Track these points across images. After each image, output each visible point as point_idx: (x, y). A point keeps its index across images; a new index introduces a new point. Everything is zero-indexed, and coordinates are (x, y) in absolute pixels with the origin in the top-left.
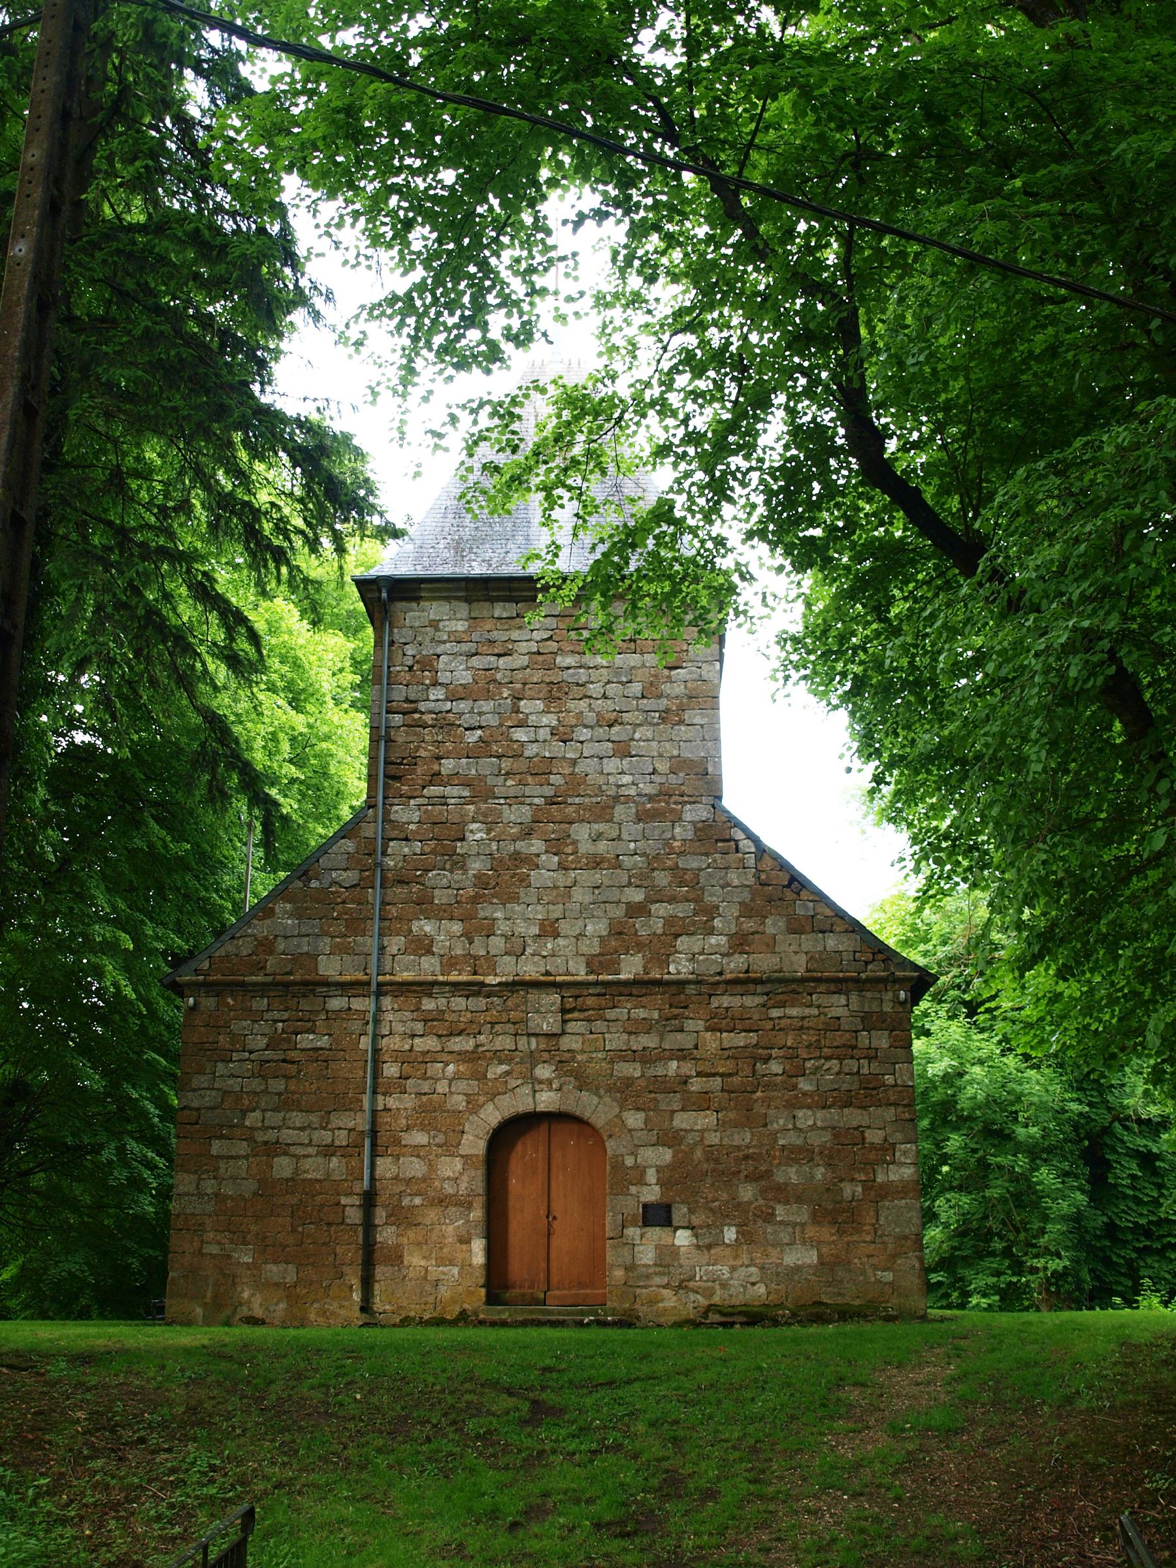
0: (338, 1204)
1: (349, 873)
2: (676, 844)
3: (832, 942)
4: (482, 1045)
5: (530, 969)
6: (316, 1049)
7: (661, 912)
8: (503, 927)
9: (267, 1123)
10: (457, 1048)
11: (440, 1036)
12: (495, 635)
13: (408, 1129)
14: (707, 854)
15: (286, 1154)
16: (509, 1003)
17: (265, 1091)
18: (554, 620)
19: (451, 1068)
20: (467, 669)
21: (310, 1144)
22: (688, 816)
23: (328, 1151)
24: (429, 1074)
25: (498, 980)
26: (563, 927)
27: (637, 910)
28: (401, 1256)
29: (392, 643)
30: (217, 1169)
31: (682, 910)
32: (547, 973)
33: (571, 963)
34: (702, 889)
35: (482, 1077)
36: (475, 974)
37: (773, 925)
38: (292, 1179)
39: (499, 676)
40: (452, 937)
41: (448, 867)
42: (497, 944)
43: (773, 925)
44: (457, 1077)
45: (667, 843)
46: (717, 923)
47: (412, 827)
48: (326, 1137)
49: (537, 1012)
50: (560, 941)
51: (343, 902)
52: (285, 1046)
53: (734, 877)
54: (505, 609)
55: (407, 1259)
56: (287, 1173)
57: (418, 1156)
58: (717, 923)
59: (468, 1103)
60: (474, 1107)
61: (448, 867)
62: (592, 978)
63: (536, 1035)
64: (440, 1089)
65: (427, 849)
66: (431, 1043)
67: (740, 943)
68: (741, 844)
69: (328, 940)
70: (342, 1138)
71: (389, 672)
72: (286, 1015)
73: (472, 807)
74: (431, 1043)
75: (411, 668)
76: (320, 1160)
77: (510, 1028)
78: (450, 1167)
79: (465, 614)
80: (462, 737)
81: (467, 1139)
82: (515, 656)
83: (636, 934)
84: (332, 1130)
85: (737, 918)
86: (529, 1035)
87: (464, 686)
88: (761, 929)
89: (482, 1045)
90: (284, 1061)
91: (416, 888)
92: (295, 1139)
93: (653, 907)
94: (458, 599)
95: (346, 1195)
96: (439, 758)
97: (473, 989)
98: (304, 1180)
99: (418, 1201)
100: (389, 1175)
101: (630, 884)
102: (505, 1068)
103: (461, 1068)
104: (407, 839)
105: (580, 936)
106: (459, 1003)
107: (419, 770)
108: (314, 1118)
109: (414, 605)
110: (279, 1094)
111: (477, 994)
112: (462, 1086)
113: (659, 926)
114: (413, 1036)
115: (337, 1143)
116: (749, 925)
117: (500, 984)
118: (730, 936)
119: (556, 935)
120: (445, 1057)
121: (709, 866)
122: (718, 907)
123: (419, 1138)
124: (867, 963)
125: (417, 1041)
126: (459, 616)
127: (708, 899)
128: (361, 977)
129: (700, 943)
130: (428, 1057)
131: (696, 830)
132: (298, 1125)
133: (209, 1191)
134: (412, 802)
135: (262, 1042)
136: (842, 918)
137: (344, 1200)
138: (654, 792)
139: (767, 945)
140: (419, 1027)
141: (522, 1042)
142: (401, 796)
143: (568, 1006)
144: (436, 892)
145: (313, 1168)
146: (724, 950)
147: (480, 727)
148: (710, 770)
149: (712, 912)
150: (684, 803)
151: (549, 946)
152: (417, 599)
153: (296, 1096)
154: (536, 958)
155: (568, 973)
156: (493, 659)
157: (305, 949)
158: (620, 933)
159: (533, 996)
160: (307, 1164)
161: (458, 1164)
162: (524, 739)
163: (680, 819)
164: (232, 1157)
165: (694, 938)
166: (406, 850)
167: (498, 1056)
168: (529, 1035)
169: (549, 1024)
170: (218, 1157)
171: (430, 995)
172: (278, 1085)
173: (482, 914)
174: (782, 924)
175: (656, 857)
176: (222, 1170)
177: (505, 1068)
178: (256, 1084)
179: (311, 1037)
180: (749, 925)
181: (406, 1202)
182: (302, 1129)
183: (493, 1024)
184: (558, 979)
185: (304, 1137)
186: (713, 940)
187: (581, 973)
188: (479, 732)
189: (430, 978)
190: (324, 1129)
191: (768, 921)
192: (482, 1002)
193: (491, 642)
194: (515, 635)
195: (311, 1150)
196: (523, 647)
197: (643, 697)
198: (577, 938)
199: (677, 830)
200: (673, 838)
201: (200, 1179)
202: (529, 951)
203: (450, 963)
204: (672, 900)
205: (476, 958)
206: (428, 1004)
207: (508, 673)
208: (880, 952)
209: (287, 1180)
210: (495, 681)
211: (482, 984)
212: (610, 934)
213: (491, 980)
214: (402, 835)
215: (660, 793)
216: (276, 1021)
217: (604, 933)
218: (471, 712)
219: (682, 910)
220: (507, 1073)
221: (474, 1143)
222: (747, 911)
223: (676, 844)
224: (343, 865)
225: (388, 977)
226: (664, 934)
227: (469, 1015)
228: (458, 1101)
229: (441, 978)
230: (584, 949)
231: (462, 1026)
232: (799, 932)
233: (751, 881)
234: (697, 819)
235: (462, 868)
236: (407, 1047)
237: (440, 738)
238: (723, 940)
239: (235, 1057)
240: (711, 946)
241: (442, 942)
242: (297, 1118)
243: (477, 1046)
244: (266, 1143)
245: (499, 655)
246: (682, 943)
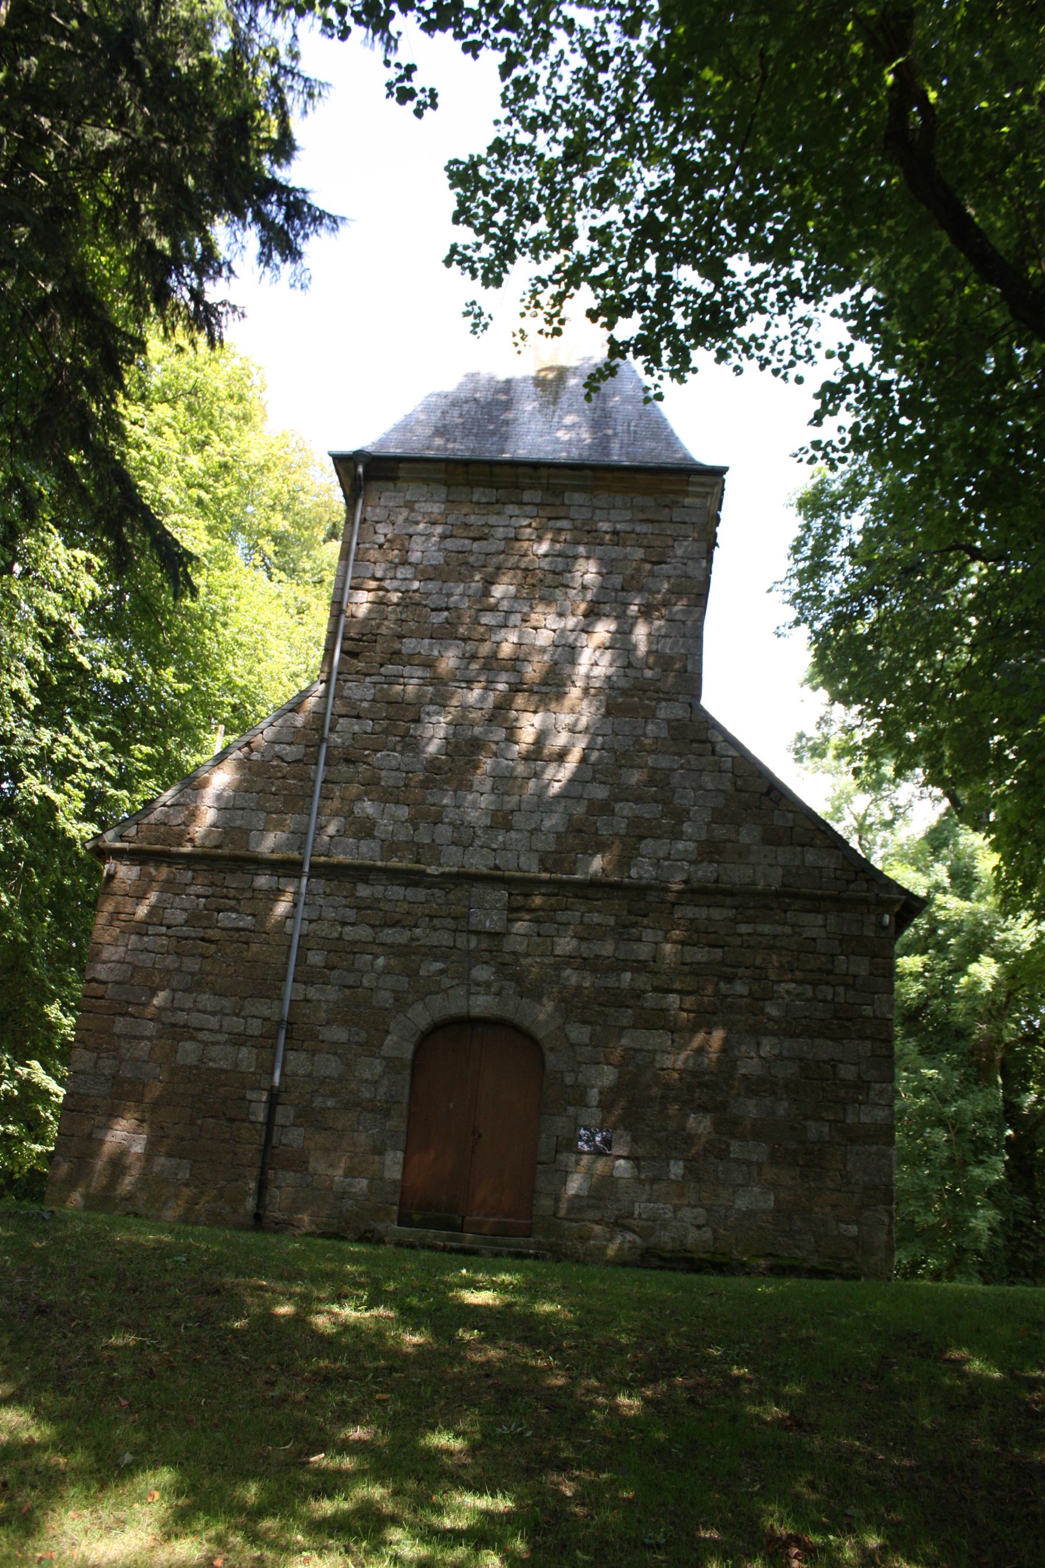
0: (243, 1098)
1: (294, 748)
2: (647, 741)
3: (811, 857)
4: (418, 940)
5: (478, 862)
6: (238, 930)
7: (625, 813)
8: (451, 815)
9: (176, 1004)
10: (389, 940)
11: (373, 926)
12: (472, 519)
13: (328, 1023)
14: (680, 755)
15: (193, 1038)
16: (451, 896)
17: (179, 970)
18: (535, 509)
19: (381, 961)
20: (439, 550)
21: (219, 1031)
22: (662, 714)
23: (239, 1040)
24: (356, 965)
25: (441, 870)
26: (517, 819)
27: (604, 808)
28: (306, 1162)
29: (364, 521)
30: (117, 1049)
31: (646, 811)
32: (497, 868)
33: (522, 859)
34: (673, 791)
35: (413, 974)
36: (418, 862)
37: (748, 835)
38: (197, 1067)
39: (472, 559)
40: (396, 822)
41: (398, 748)
42: (444, 833)
43: (748, 835)
44: (387, 971)
45: (637, 740)
46: (687, 828)
47: (365, 704)
48: (236, 1024)
49: (481, 907)
50: (513, 835)
51: (284, 777)
52: (205, 923)
53: (708, 781)
54: (485, 495)
55: (312, 1165)
56: (192, 1060)
57: (335, 1054)
58: (687, 828)
59: (396, 1000)
60: (401, 1003)
61: (398, 748)
62: (545, 876)
63: (477, 933)
64: (366, 982)
65: (378, 728)
66: (364, 933)
67: (710, 850)
68: (718, 748)
69: (263, 815)
70: (255, 1027)
71: (358, 549)
72: (209, 891)
73: (430, 689)
74: (364, 933)
75: (381, 546)
76: (229, 1049)
77: (451, 923)
78: (370, 1069)
79: (444, 496)
80: (427, 616)
81: (391, 1040)
82: (491, 540)
83: (596, 833)
84: (245, 1018)
85: (709, 824)
86: (470, 932)
87: (435, 567)
88: (733, 836)
89: (418, 940)
90: (203, 939)
91: (362, 767)
92: (187, 934)
93: (618, 806)
94: (437, 481)
95: (253, 1089)
96: (401, 637)
97: (410, 878)
98: (210, 1069)
99: (330, 1103)
100: (301, 1072)
101: (594, 779)
102: (439, 965)
103: (393, 962)
104: (358, 717)
105: (535, 831)
106: (397, 892)
107: (378, 648)
108: (227, 1003)
109: (391, 485)
110: (193, 974)
111: (416, 884)
112: (390, 981)
113: (622, 826)
114: (344, 924)
115: (249, 1032)
116: (720, 832)
117: (443, 875)
118: (699, 843)
119: (509, 827)
120: (377, 950)
121: (681, 767)
122: (688, 812)
123: (338, 1034)
124: (849, 882)
125: (349, 928)
126: (436, 498)
127: (677, 801)
128: (295, 855)
129: (666, 848)
130: (355, 948)
131: (670, 728)
132: (209, 1009)
133: (107, 1072)
134: (368, 679)
135: (181, 917)
136: (824, 832)
137: (250, 1095)
138: (627, 686)
139: (740, 854)
140: (351, 915)
141: (461, 941)
142: (357, 673)
143: (514, 904)
144: (383, 773)
145: (221, 1057)
146: (693, 857)
147: (447, 609)
148: (689, 667)
149: (681, 815)
150: (659, 700)
151: (501, 838)
152: (394, 479)
153: (211, 978)
154: (485, 851)
155: (520, 870)
156: (467, 542)
157: (238, 823)
158: (580, 831)
159: (478, 890)
160: (214, 1052)
161: (378, 1066)
162: (493, 623)
163: (654, 716)
164: (135, 1037)
165: (659, 842)
166: (356, 728)
167: (434, 952)
168: (470, 932)
169: (491, 922)
170: (119, 1036)
171: (366, 882)
172: (192, 965)
173: (430, 800)
174: (757, 833)
175: (625, 754)
176: (123, 1051)
177: (439, 965)
178: (171, 962)
179: (234, 916)
180: (720, 832)
181: (318, 1103)
182: (213, 1013)
183: (431, 917)
184: (507, 873)
185: (213, 1022)
186: (680, 845)
187: (531, 868)
188: (446, 614)
189: (368, 862)
190: (237, 1015)
191: (743, 831)
192: (421, 894)
193: (466, 526)
194: (493, 520)
195: (222, 1038)
196: (500, 532)
197: (623, 589)
198: (532, 832)
199: (650, 727)
200: (645, 735)
201: (99, 1058)
202: (478, 842)
203: (391, 848)
204: (639, 800)
205: (419, 845)
206: (363, 891)
207: (483, 557)
208: (864, 871)
209: (191, 1067)
210: (467, 563)
211: (423, 873)
212: (567, 831)
213: (432, 870)
214: (354, 713)
215: (635, 688)
216: (198, 896)
217: (561, 830)
218: (440, 592)
219: (646, 811)
220: (442, 972)
221: (398, 1043)
222: (719, 816)
223: (647, 741)
224: (288, 739)
225: (323, 859)
226: (627, 835)
227: (406, 906)
228: (385, 998)
229: (379, 863)
230: (540, 846)
231: (397, 917)
232: (778, 844)
233: (728, 786)
234: (672, 716)
235: (413, 750)
236: (335, 935)
237: (404, 616)
238: (691, 846)
239: (152, 930)
240: (678, 851)
241: (385, 827)
242: (206, 999)
243: (412, 940)
244: (174, 1025)
245: (474, 539)
246: (648, 846)
